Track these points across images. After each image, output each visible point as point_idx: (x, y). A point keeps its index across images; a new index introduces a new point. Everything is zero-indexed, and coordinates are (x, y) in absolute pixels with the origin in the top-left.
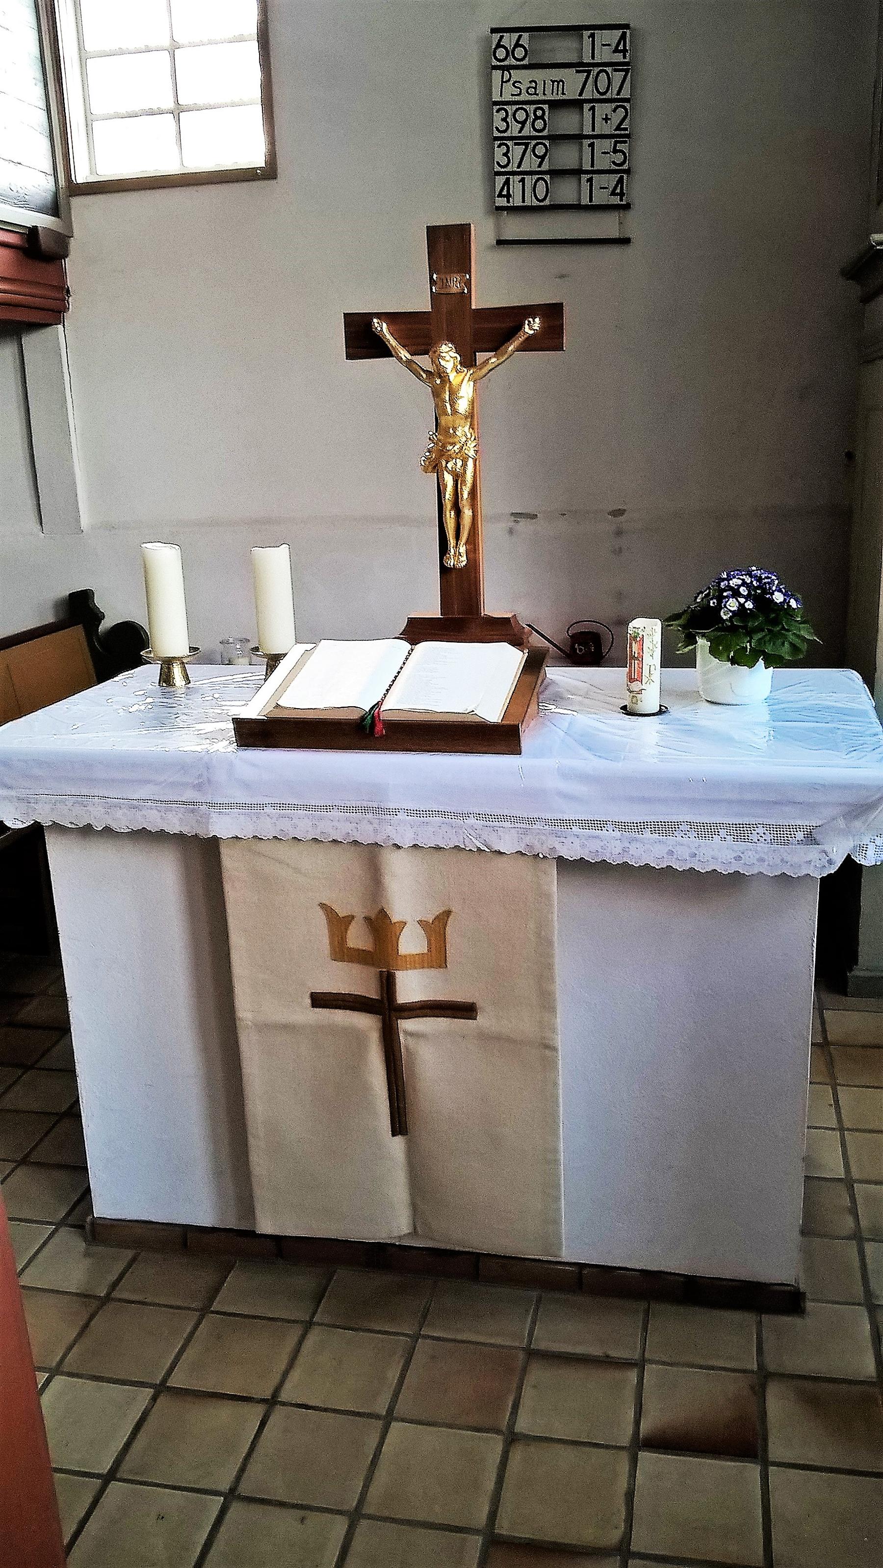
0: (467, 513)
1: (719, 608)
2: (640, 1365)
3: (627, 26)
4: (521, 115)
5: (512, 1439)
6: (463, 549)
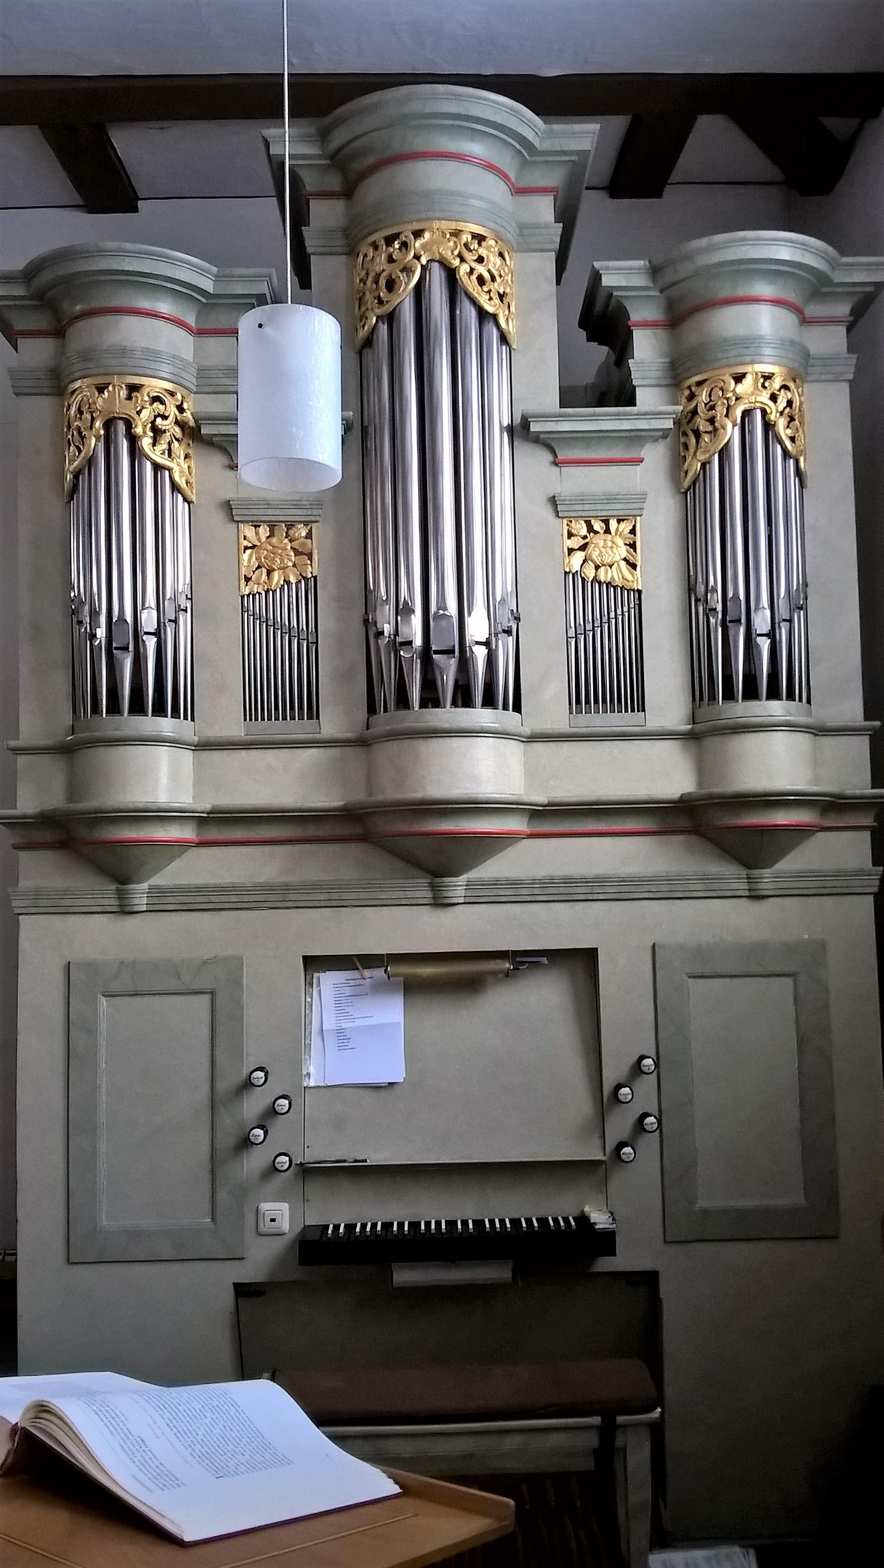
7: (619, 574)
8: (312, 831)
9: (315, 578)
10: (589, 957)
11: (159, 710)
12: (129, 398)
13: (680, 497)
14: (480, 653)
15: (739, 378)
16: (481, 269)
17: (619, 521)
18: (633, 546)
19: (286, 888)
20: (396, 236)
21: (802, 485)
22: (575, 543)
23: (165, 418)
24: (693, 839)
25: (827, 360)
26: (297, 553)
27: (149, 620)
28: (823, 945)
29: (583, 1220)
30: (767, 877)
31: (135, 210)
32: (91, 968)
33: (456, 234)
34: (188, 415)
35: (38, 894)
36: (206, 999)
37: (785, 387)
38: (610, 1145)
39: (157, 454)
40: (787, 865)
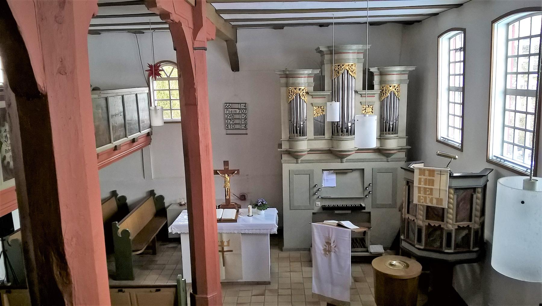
0: (229, 193)
1: (258, 204)
2: (252, 290)
3: (246, 103)
4: (230, 116)
6: (228, 196)
8: (325, 152)
10: (363, 170)
11: (303, 136)
12: (299, 90)
13: (380, 103)
14: (350, 128)
15: (390, 86)
16: (352, 70)
18: (373, 109)
19: (320, 160)
20: (340, 65)
21: (399, 100)
22: (364, 109)
23: (304, 92)
24: (379, 153)
26: (322, 111)
27: (302, 123)
29: (361, 205)
30: (389, 159)
31: (283, 29)
32: (293, 171)
33: (349, 65)
34: (306, 91)
35: (285, 160)
38: (365, 195)
40: (393, 157)
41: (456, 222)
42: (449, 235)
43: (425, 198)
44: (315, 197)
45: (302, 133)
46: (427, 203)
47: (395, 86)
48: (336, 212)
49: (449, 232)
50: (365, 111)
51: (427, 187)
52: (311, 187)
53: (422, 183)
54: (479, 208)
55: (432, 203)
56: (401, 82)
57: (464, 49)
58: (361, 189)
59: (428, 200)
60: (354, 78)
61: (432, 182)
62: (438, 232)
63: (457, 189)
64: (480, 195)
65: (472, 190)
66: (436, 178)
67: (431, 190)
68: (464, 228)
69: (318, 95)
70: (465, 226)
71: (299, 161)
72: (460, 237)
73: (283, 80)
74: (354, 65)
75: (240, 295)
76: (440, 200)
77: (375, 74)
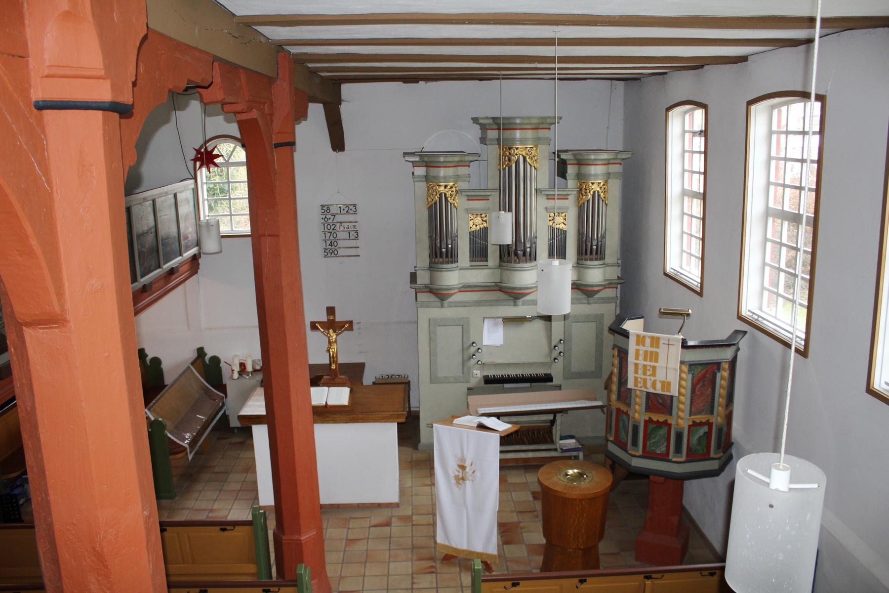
2: (370, 517)
5: (349, 529)
7: (562, 226)
9: (487, 227)
14: (528, 250)
15: (593, 184)
17: (562, 213)
18: (565, 219)
22: (551, 218)
25: (615, 174)
28: (603, 315)
34: (457, 188)
36: (461, 327)
37: (604, 185)
38: (552, 358)
39: (452, 201)
41: (691, 414)
42: (679, 436)
43: (645, 381)
44: (473, 362)
45: (451, 256)
46: (647, 389)
47: (600, 183)
48: (507, 386)
49: (679, 430)
50: (552, 221)
51: (648, 363)
52: (465, 346)
53: (641, 358)
54: (723, 392)
55: (655, 388)
56: (608, 176)
57: (705, 133)
58: (545, 349)
59: (649, 384)
60: (535, 169)
61: (655, 357)
62: (663, 431)
63: (692, 366)
64: (726, 374)
65: (715, 367)
66: (662, 350)
67: (654, 368)
68: (701, 424)
69: (475, 196)
70: (704, 421)
71: (446, 303)
72: (697, 437)
73: (420, 171)
74: (535, 149)
75: (350, 526)
76: (666, 385)
77: (568, 162)
